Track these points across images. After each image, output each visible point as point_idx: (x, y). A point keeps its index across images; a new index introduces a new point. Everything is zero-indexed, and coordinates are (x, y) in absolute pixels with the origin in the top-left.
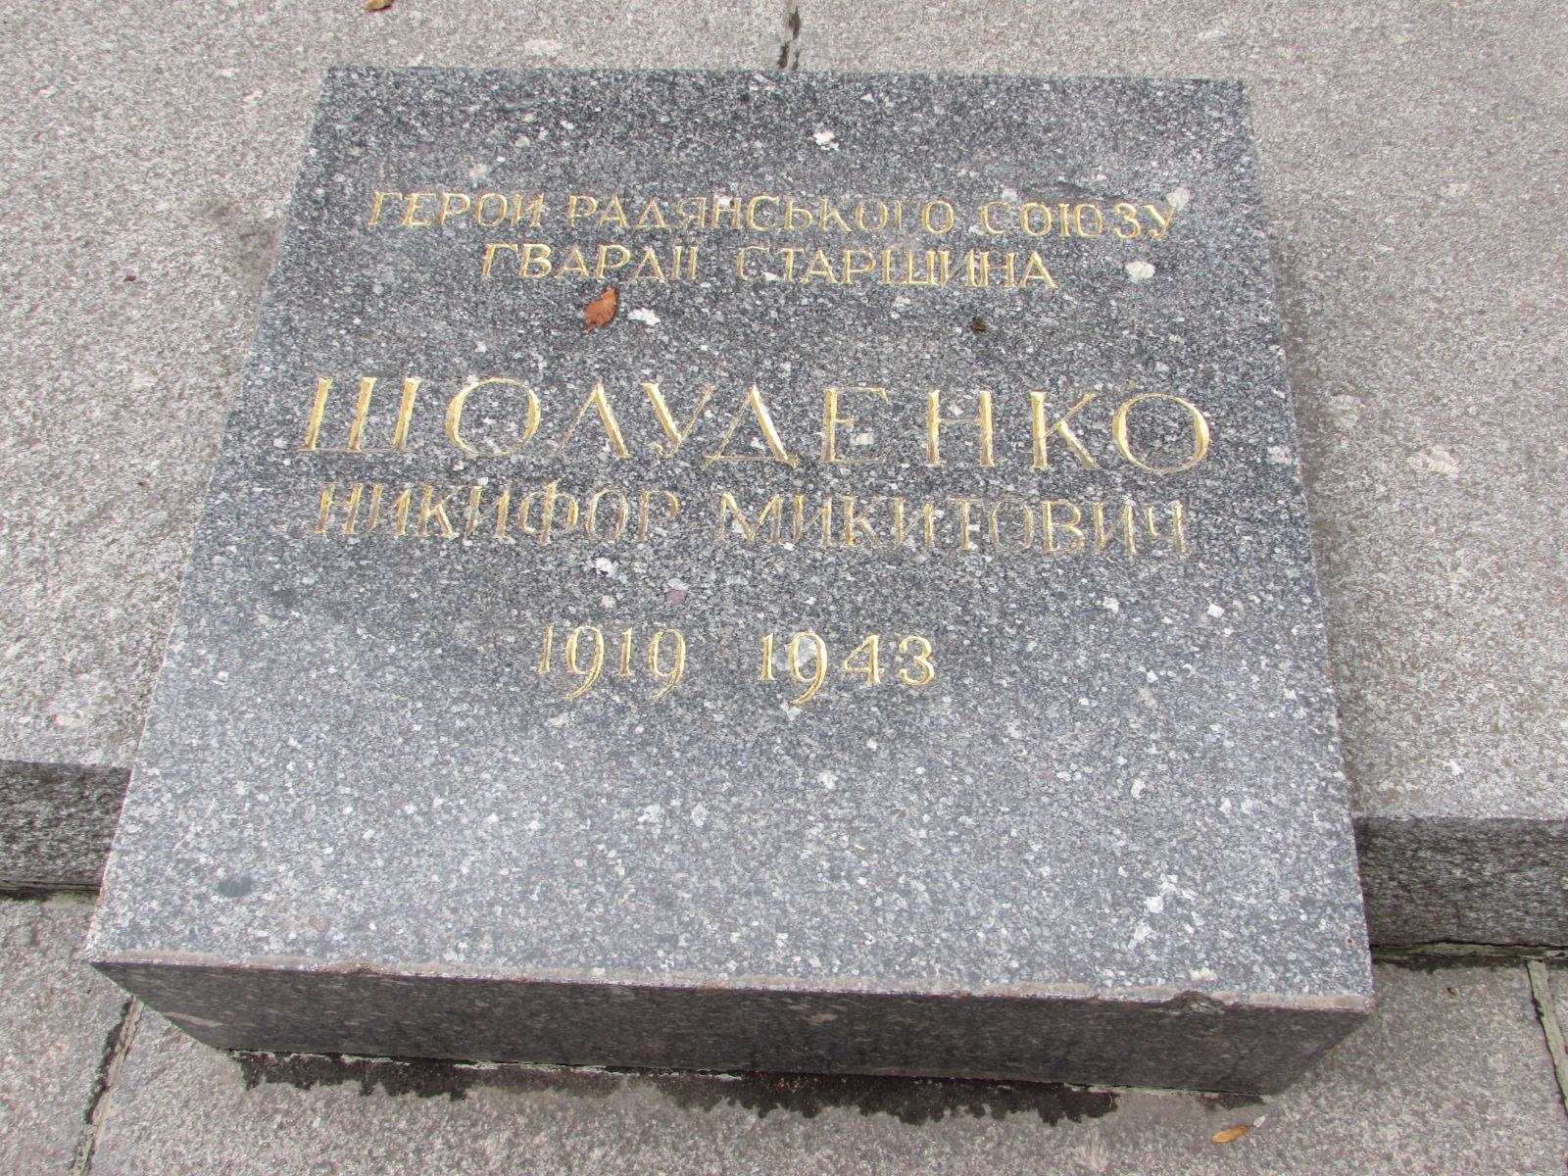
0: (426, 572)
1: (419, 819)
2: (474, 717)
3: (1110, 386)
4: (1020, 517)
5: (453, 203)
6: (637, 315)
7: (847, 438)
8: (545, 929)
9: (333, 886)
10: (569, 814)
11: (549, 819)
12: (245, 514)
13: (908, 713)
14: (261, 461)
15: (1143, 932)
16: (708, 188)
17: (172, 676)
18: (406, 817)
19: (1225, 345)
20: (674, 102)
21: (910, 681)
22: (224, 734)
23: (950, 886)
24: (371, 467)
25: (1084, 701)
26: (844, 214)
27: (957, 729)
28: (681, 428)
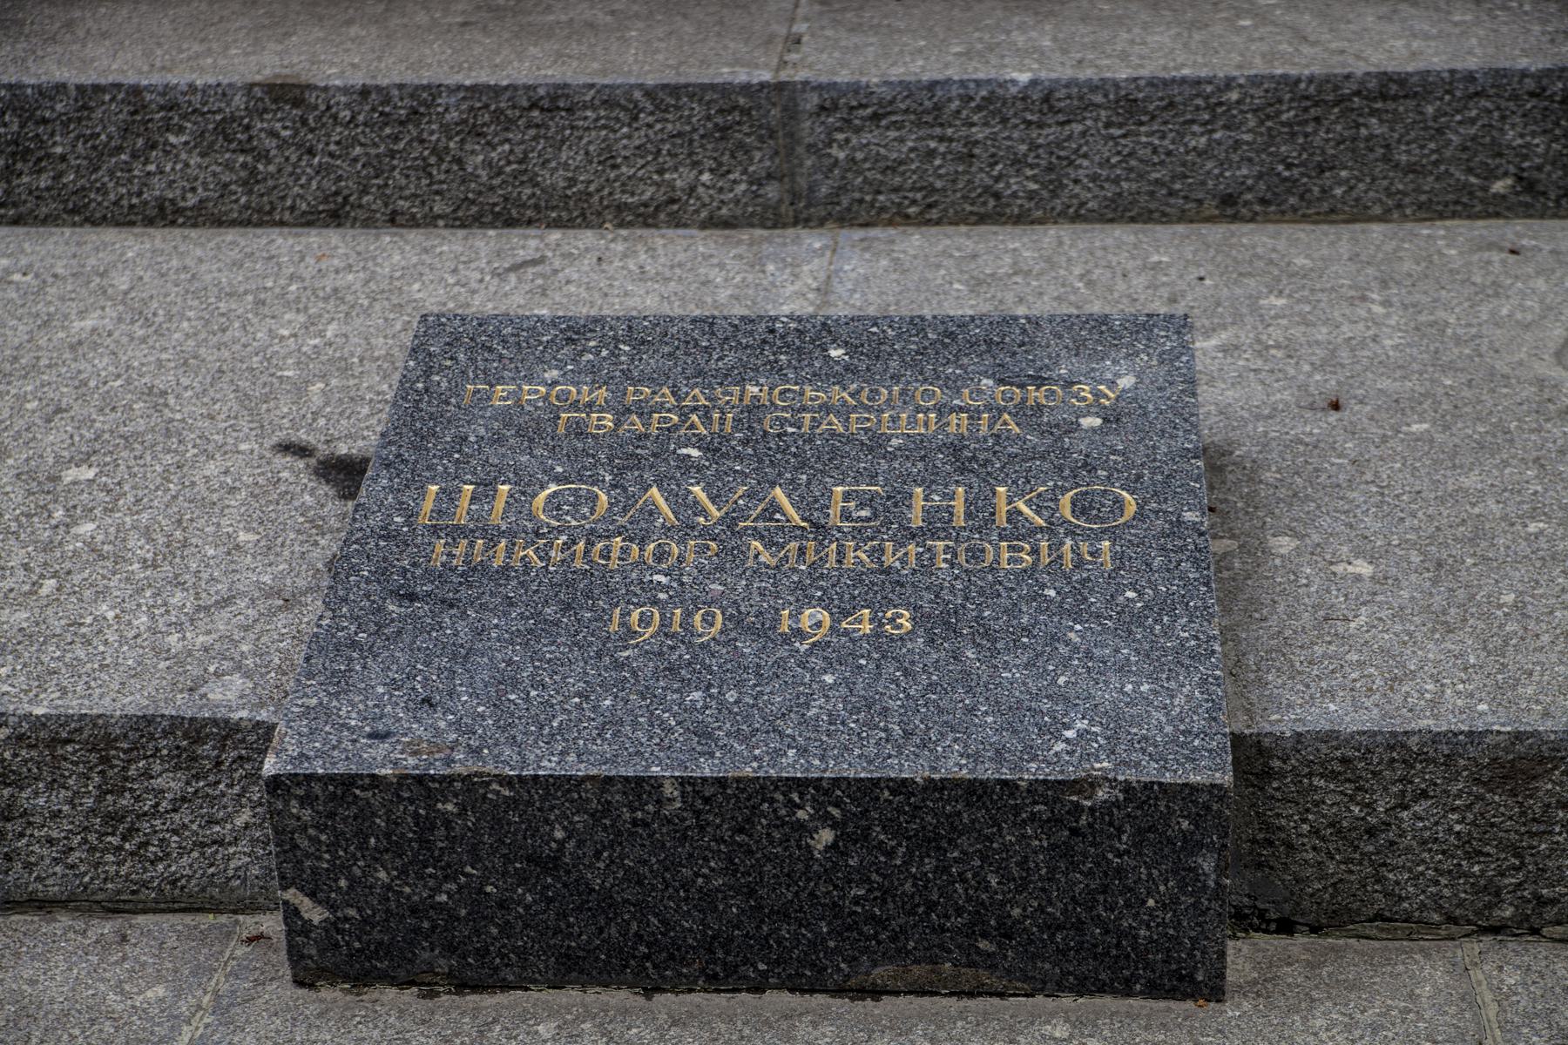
4: (983, 551)
5: (532, 392)
6: (684, 451)
14: (382, 528)
15: (1060, 746)
16: (741, 382)
20: (713, 334)
24: (472, 531)
25: (1025, 640)
26: (852, 395)
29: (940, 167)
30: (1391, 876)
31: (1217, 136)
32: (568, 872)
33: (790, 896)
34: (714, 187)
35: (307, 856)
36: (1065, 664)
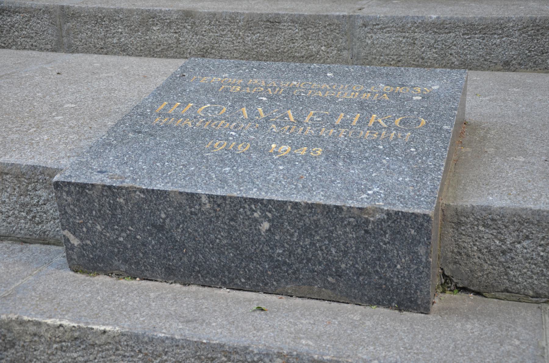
6: (261, 98)
26: (330, 86)
29: (403, 47)
30: (511, 273)
31: (504, 39)
32: (167, 232)
33: (253, 251)
34: (325, 52)
35: (71, 217)
36: (377, 170)
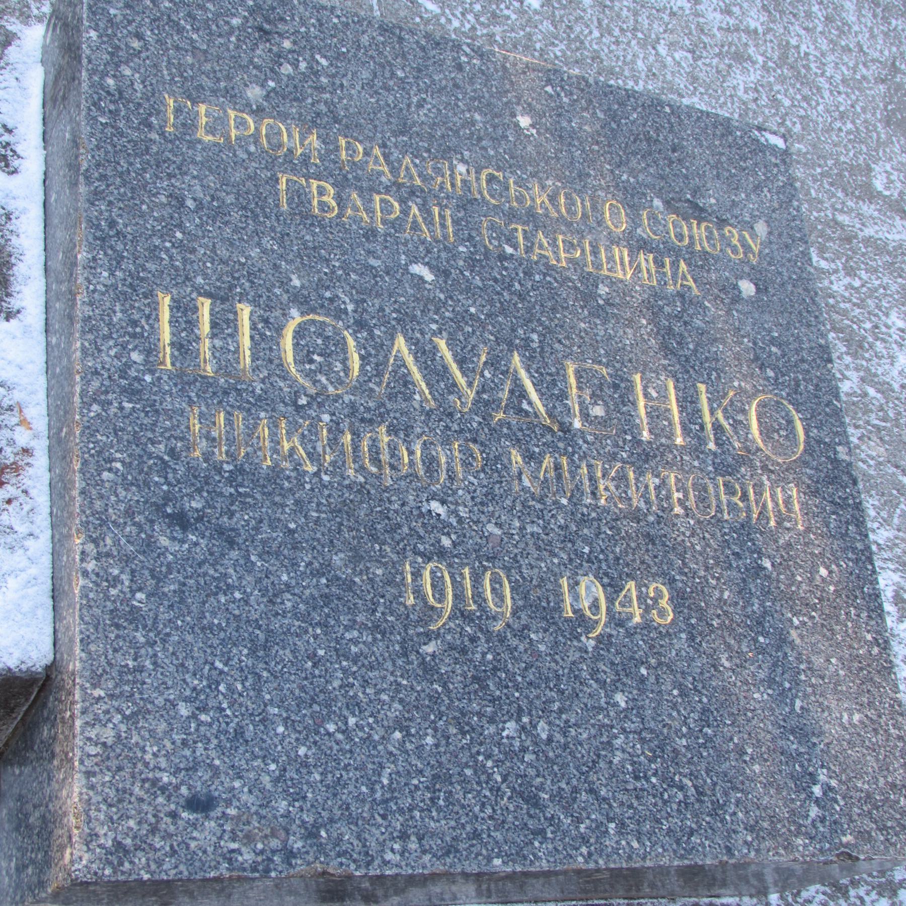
0: (297, 502)
1: (340, 736)
2: (364, 643)
3: (743, 384)
7: (587, 408)
8: (454, 828)
9: (284, 799)
10: (453, 730)
11: (439, 735)
12: (122, 430)
13: (662, 646)
14: (123, 374)
17: (91, 595)
18: (329, 734)
19: (803, 361)
21: (659, 620)
22: (155, 655)
23: (705, 782)
25: (761, 639)
27: (693, 659)
28: (470, 384)
